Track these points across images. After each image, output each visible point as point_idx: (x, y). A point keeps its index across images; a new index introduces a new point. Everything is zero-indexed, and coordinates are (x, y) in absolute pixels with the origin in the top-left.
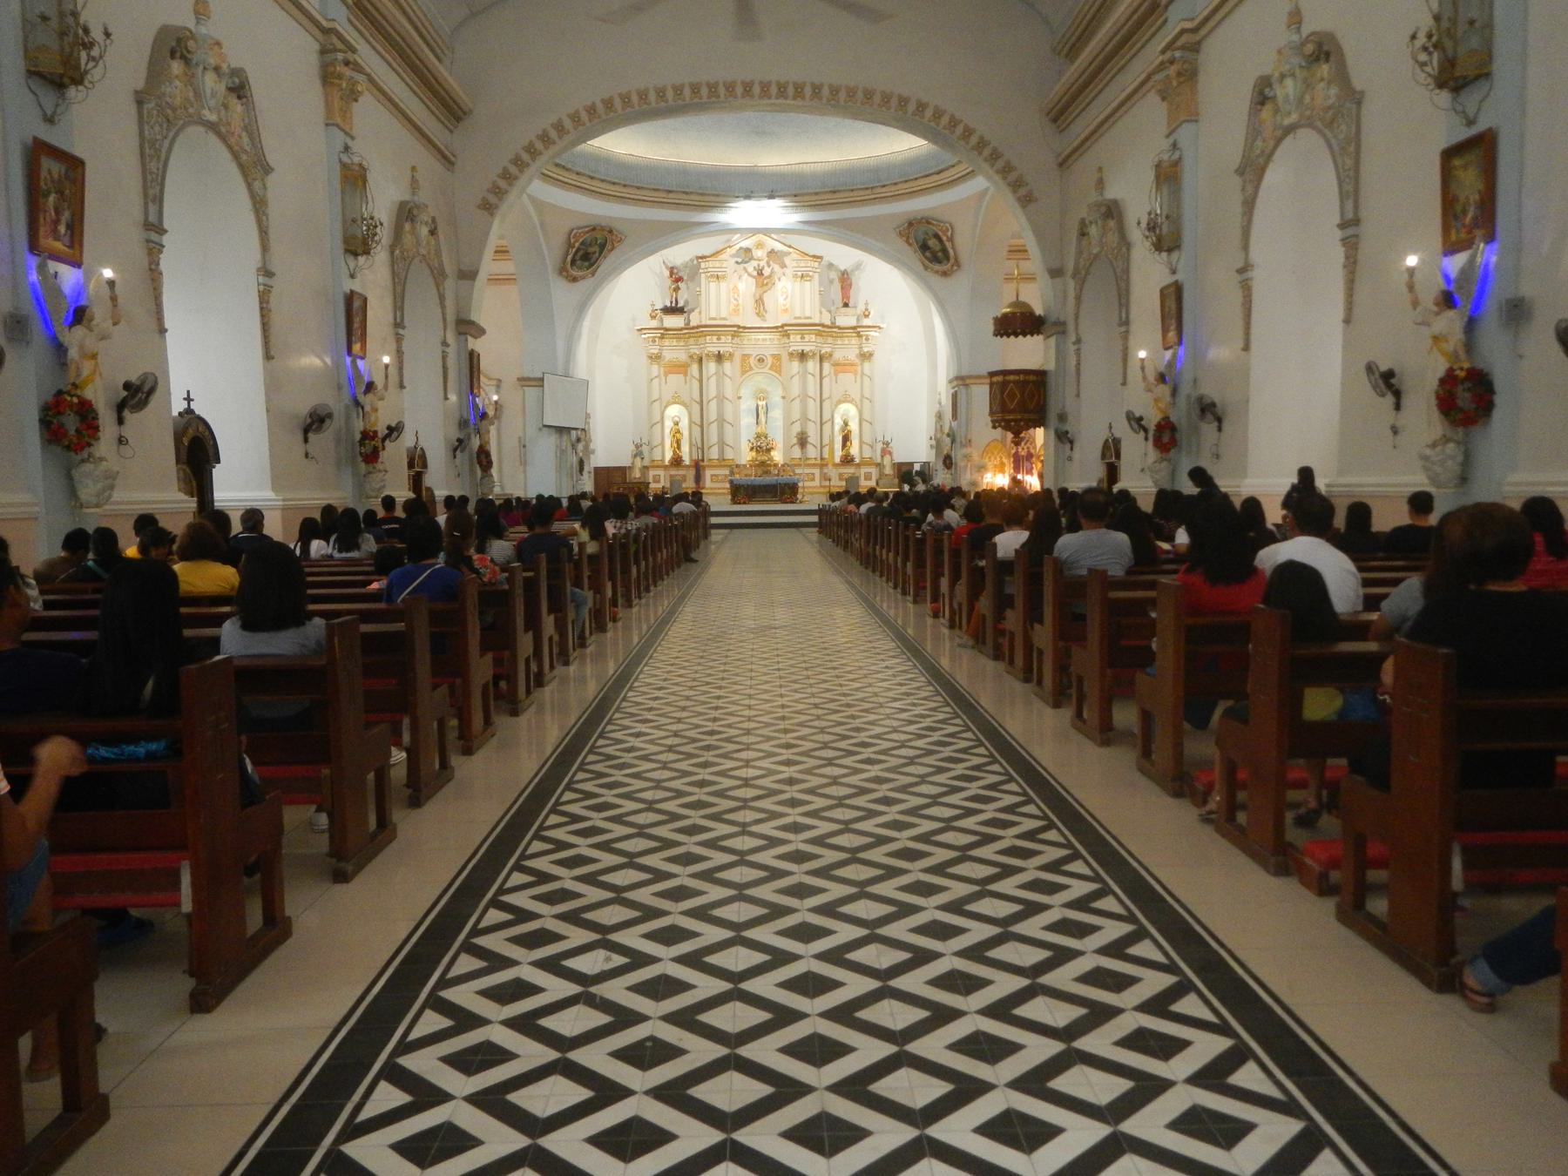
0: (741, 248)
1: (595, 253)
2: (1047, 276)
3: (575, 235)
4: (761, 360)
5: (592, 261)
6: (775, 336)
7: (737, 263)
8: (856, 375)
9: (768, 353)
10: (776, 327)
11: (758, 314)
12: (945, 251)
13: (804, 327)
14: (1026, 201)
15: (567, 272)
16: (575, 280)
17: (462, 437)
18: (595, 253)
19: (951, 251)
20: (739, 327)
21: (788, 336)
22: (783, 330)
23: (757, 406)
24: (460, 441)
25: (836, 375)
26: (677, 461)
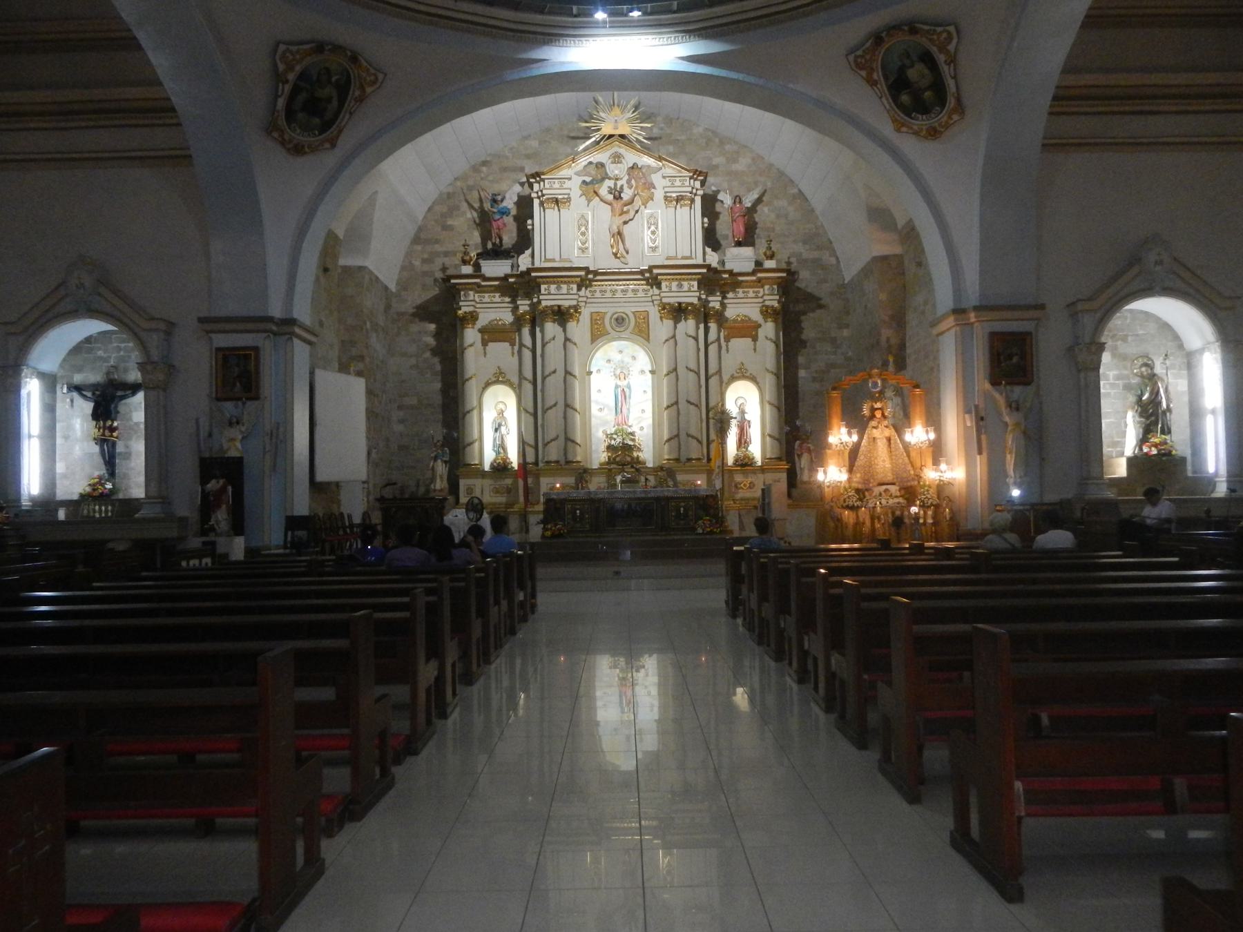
0: (590, 163)
3: (283, 56)
4: (620, 321)
6: (642, 286)
7: (584, 182)
8: (755, 339)
9: (629, 310)
10: (642, 272)
11: (615, 255)
13: (679, 271)
15: (282, 132)
16: (298, 150)
18: (329, 100)
19: (951, 84)
20: (586, 269)
21: (659, 286)
22: (652, 278)
23: (617, 387)
25: (727, 340)
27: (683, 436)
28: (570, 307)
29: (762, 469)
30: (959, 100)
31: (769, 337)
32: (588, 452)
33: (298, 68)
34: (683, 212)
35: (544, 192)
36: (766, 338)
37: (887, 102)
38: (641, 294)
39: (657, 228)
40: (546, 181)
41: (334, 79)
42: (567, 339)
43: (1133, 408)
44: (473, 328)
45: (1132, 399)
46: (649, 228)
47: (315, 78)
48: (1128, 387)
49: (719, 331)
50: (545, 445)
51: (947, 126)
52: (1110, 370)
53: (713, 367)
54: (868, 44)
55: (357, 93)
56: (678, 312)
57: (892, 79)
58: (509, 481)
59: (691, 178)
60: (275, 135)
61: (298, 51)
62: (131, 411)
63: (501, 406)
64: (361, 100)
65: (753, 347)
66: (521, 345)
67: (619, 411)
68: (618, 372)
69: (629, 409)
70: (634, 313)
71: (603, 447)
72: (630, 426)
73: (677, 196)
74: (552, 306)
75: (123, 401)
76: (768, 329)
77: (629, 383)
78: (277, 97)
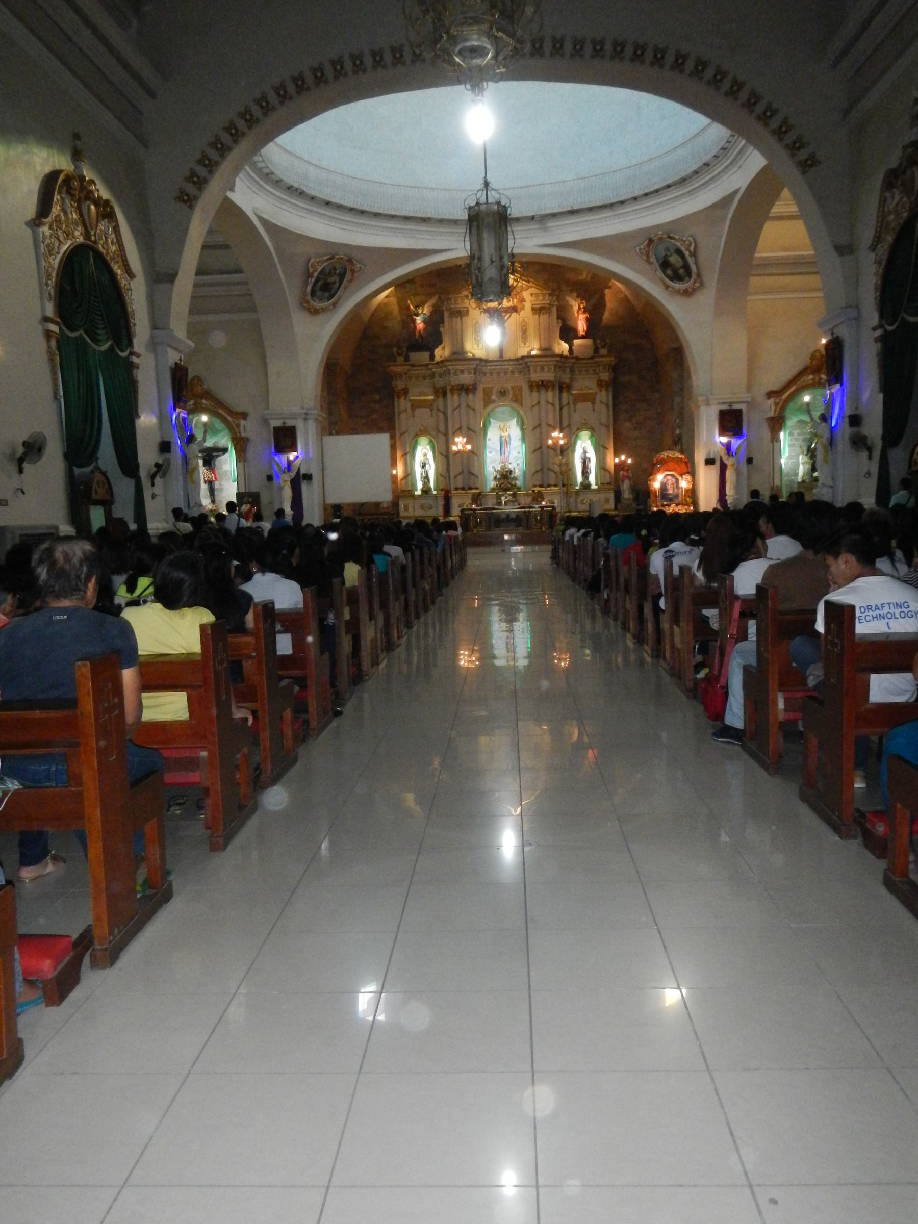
1: (334, 283)
2: (835, 254)
5: (333, 292)
8: (593, 402)
9: (509, 385)
10: (517, 359)
12: (686, 267)
14: (807, 165)
15: (308, 302)
16: (315, 312)
17: (160, 462)
18: (334, 283)
19: (694, 268)
23: (501, 437)
24: (157, 465)
25: (575, 404)
26: (426, 491)
27: (545, 469)
28: (470, 385)
29: (598, 491)
30: (699, 275)
31: (603, 401)
32: (485, 480)
33: (319, 269)
34: (544, 318)
35: (452, 306)
36: (601, 402)
37: (660, 273)
38: (516, 375)
39: (526, 329)
40: (453, 299)
41: (337, 272)
42: (468, 406)
43: (803, 453)
44: (405, 399)
45: (805, 449)
46: (522, 328)
47: (328, 271)
48: (804, 440)
49: (568, 398)
50: (455, 477)
51: (694, 290)
52: (796, 430)
53: (565, 423)
54: (646, 242)
55: (350, 278)
56: (542, 386)
57: (661, 262)
58: (430, 501)
59: (550, 295)
60: (305, 305)
61: (320, 261)
62: (222, 464)
63: (425, 451)
64: (351, 280)
65: (592, 408)
66: (438, 410)
67: (503, 453)
68: (502, 426)
69: (509, 452)
70: (512, 388)
71: (492, 477)
72: (510, 463)
73: (541, 307)
74: (458, 385)
75: (220, 458)
76: (604, 396)
77: (509, 434)
78: (306, 284)
